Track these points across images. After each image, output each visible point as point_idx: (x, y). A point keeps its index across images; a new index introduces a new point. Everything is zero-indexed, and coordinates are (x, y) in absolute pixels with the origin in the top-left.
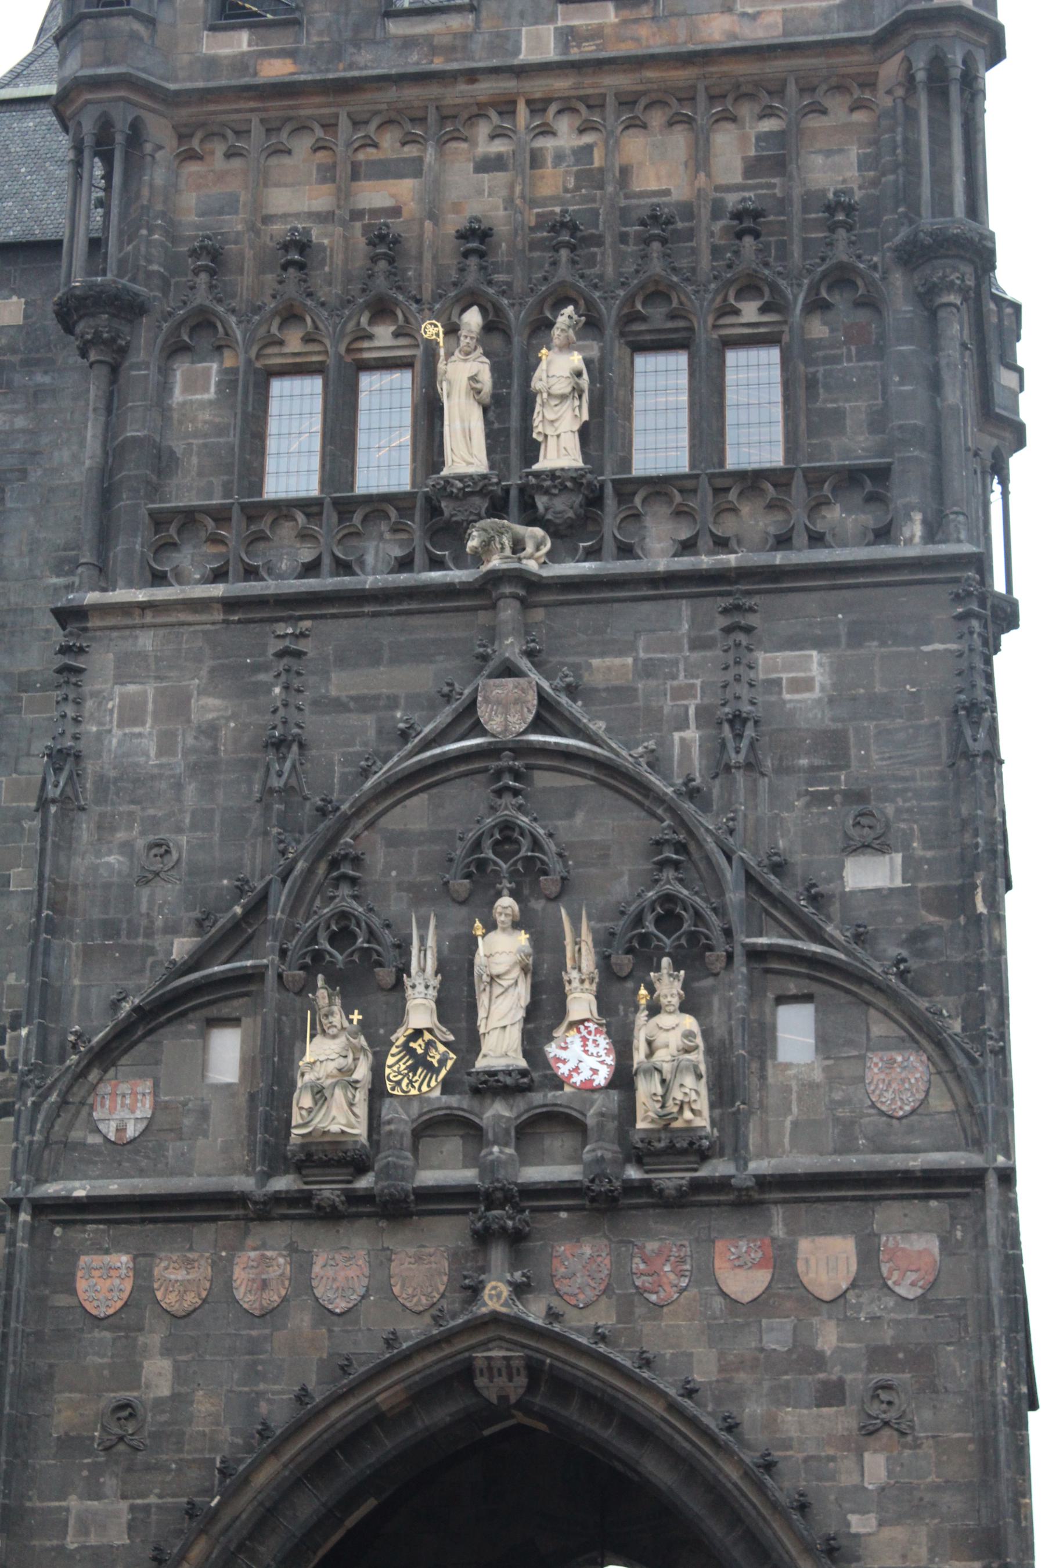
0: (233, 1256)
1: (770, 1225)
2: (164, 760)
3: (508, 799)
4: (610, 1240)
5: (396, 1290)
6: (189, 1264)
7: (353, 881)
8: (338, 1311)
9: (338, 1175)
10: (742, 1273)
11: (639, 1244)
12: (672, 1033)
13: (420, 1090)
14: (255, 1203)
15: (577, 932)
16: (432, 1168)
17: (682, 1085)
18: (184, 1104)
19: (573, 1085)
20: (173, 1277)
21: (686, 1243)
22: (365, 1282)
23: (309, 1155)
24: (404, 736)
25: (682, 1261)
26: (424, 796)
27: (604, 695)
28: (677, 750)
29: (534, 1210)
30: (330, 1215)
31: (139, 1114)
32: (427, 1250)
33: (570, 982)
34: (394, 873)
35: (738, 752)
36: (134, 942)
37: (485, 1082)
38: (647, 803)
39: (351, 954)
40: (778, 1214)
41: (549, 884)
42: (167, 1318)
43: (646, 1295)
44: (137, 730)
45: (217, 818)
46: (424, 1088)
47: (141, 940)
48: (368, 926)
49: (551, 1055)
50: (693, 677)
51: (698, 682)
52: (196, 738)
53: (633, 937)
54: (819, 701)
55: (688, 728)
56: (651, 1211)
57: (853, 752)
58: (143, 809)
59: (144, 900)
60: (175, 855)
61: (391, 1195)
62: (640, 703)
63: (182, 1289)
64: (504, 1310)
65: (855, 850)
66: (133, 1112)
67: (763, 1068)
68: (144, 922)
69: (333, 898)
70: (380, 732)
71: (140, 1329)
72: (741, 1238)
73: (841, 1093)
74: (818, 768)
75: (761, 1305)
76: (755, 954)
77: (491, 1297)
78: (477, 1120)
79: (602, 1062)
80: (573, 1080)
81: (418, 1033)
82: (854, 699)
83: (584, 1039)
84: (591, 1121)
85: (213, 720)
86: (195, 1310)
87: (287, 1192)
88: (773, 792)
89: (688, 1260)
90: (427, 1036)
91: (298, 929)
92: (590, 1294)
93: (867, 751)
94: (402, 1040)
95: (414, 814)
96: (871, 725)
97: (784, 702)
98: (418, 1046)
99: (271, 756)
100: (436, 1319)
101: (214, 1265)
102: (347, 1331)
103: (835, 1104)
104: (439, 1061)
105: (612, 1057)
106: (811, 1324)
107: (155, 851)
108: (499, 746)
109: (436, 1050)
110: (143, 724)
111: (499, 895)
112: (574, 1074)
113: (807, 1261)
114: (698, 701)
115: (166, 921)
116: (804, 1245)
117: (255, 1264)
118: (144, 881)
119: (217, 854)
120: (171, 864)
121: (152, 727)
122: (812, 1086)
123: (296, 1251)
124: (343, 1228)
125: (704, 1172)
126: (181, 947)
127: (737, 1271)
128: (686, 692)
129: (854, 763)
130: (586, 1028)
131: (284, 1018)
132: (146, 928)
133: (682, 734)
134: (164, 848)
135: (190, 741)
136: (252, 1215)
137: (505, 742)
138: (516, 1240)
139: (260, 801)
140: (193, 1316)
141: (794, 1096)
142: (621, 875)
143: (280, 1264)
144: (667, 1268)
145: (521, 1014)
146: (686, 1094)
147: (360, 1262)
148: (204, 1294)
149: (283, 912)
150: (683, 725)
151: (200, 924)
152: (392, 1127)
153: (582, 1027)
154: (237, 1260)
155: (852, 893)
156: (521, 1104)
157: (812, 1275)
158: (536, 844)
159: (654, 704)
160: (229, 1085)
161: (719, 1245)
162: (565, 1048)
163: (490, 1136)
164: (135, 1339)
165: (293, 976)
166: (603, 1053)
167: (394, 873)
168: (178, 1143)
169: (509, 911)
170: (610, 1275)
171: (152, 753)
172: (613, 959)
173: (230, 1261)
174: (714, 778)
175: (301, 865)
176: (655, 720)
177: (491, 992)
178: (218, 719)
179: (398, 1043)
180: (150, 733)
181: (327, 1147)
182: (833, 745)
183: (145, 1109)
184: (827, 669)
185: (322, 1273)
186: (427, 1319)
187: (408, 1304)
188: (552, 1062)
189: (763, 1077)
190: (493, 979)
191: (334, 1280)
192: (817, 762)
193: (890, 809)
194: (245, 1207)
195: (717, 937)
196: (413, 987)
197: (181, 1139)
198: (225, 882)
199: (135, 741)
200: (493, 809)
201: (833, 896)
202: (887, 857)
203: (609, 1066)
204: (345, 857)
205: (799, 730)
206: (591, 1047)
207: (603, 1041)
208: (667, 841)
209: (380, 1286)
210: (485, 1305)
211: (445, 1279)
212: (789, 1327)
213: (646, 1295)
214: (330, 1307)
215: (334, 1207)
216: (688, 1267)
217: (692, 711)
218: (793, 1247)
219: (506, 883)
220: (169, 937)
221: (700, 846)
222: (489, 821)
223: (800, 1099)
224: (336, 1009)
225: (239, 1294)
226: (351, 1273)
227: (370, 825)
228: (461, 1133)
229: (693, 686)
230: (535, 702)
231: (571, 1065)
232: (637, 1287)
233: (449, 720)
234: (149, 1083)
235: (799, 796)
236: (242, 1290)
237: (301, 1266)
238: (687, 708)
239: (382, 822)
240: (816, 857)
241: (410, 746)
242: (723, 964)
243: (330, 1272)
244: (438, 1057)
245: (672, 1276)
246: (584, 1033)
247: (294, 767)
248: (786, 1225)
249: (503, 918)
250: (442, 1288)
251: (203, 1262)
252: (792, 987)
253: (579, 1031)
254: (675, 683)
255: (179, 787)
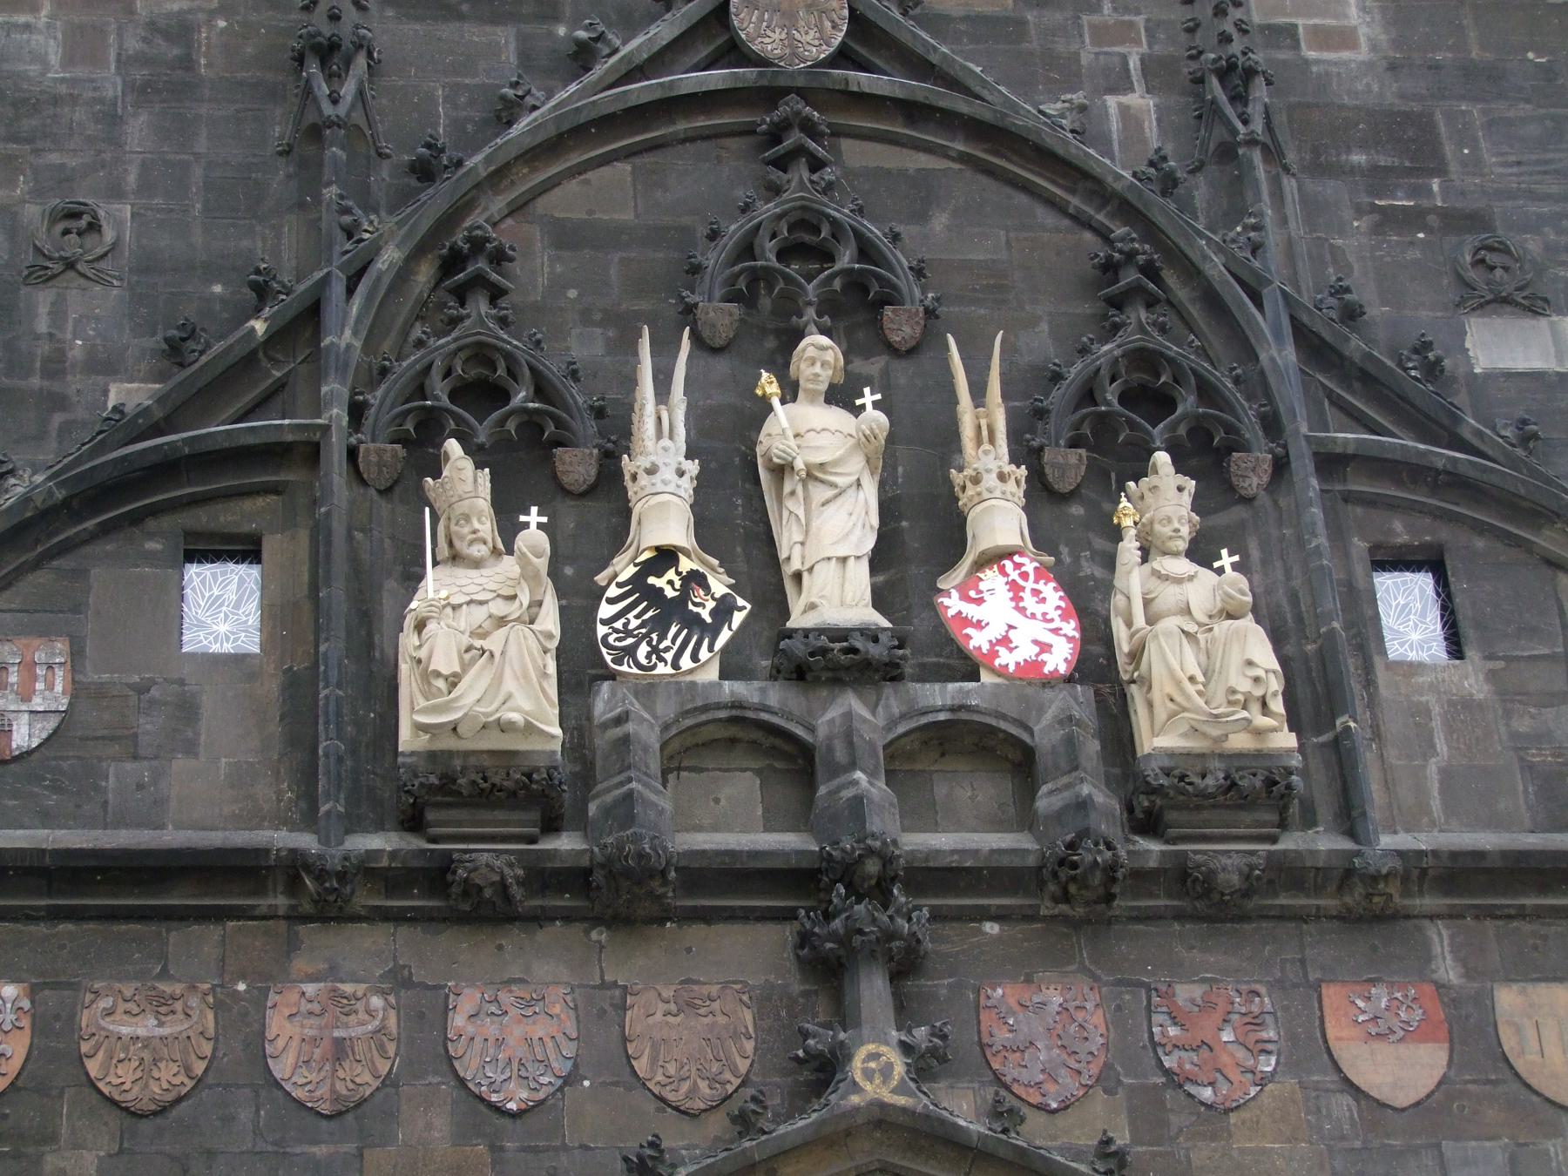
0: (265, 993)
1: (1429, 958)
2: (80, 72)
3: (801, 171)
4: (1096, 979)
5: (641, 1066)
6: (161, 1005)
7: (496, 294)
8: (512, 1106)
9: (506, 824)
10: (1383, 1050)
11: (1163, 988)
12: (1188, 586)
13: (675, 665)
14: (321, 875)
15: (978, 393)
16: (699, 829)
17: (1250, 663)
18: (142, 689)
19: (1001, 672)
20: (125, 1030)
21: (1262, 990)
22: (569, 1050)
23: (448, 780)
24: (583, 56)
25: (1256, 1022)
26: (623, 168)
27: (963, 27)
28: (1115, 125)
29: (937, 916)
30: (483, 910)
31: (38, 703)
32: (705, 990)
33: (976, 480)
34: (572, 294)
35: (1245, 122)
36: (22, 384)
37: (824, 651)
38: (1075, 202)
39: (502, 422)
40: (1440, 938)
41: (901, 325)
42: (114, 1119)
43: (1188, 1087)
44: (22, 19)
45: (198, 173)
46: (686, 662)
47: (36, 382)
48: (532, 369)
49: (951, 613)
50: (1127, 10)
51: (1140, 20)
52: (144, 39)
53: (1082, 420)
54: (1370, 65)
55: (1132, 90)
56: (1177, 926)
57: (1448, 149)
58: (37, 152)
59: (43, 310)
60: (109, 235)
61: (641, 855)
62: (1035, 45)
63: (147, 1055)
64: (901, 1101)
65: (1481, 306)
66: (27, 699)
67: (1368, 669)
68: (44, 348)
69: (454, 322)
70: (525, 58)
71: (51, 1138)
72: (1372, 982)
73: (1527, 721)
74: (1388, 170)
75: (1434, 1114)
76: (1330, 463)
77: (868, 1074)
78: (800, 732)
79: (1056, 631)
80: (997, 662)
81: (666, 557)
82: (1435, 67)
83: (1015, 588)
84: (1044, 735)
85: (181, 12)
86: (179, 1100)
87: (394, 854)
88: (1313, 209)
89: (1269, 1019)
90: (686, 565)
91: (384, 372)
92: (1070, 1085)
93: (1475, 148)
94: (631, 570)
95: (605, 192)
96: (1475, 112)
97: (1307, 62)
98: (666, 583)
99: (313, 68)
100: (744, 1123)
101: (218, 1007)
102: (535, 1150)
103: (1520, 743)
104: (713, 613)
105: (1073, 624)
106: (1547, 1152)
107: (60, 227)
108: (782, 82)
109: (707, 588)
110: (35, 9)
111: (799, 335)
112: (1002, 651)
113: (1518, 1030)
114: (1145, 48)
115: (90, 351)
116: (1507, 998)
117: (316, 1007)
118: (40, 275)
119: (198, 238)
120: (100, 251)
121: (52, 16)
122: (1468, 704)
123: (408, 983)
124: (512, 939)
125: (1289, 842)
126: (129, 393)
127: (1377, 1045)
128: (1125, 33)
129: (1453, 167)
130: (1018, 566)
131: (358, 535)
132: (46, 361)
133: (1123, 99)
134: (86, 219)
135: (133, 45)
136: (307, 907)
137: (792, 75)
138: (905, 966)
139: (287, 153)
140: (175, 1113)
141: (1437, 723)
142: (1033, 322)
143: (377, 1010)
144: (1227, 1036)
145: (870, 543)
146: (1257, 680)
147: (557, 1009)
148: (199, 1068)
149: (355, 333)
150: (1121, 84)
151: (175, 351)
152: (630, 727)
153: (1008, 564)
154: (273, 998)
155: (1490, 376)
156: (893, 700)
157: (1532, 1056)
158: (866, 250)
159: (1060, 47)
160: (238, 659)
161: (1331, 994)
162: (980, 601)
163: (840, 755)
164: (38, 1161)
165: (379, 452)
166: (1055, 615)
167: (572, 294)
168: (129, 766)
169: (829, 356)
170: (1106, 1045)
171: (54, 59)
172: (1048, 456)
173: (259, 1001)
174: (1192, 172)
175: (390, 256)
176: (1067, 74)
177: (806, 499)
178: (190, 11)
179: (622, 578)
180: (48, 26)
181: (487, 762)
182: (1411, 141)
183: (53, 693)
184: (1378, 17)
185: (471, 1029)
186: (717, 1125)
187: (671, 1097)
188: (953, 629)
189: (1369, 682)
190: (813, 475)
191: (499, 1042)
192: (1383, 161)
193: (1533, 245)
194: (293, 885)
195: (1251, 429)
196: (652, 471)
197: (135, 757)
198: (218, 289)
199: (16, 36)
200: (775, 190)
201: (1454, 379)
202: (1543, 323)
203: (1070, 639)
204: (478, 244)
205: (1342, 107)
206: (1029, 601)
207: (1053, 596)
208: (1130, 256)
209: (607, 1056)
210: (856, 1087)
211: (749, 1046)
212: (1501, 1158)
213: (1188, 1087)
214: (494, 1098)
215: (503, 887)
216: (1272, 1034)
217: (1134, 63)
218: (1484, 1003)
219: (811, 313)
220: (100, 379)
221: (1191, 272)
222: (767, 210)
223: (1450, 730)
224: (484, 503)
225: (280, 1069)
226: (539, 1030)
227: (517, 209)
228: (756, 765)
229: (1131, 24)
230: (846, 12)
231: (995, 631)
232: (1167, 1072)
233: (676, 32)
234: (61, 645)
235: (1359, 211)
236: (290, 1059)
237: (421, 1015)
238: (1124, 59)
239: (541, 205)
240: (1407, 312)
241: (589, 78)
242: (1266, 479)
243: (491, 1028)
244: (711, 604)
245: (1241, 1054)
246: (1014, 575)
247: (361, 93)
248: (1462, 961)
249: (817, 369)
250: (743, 1066)
251: (194, 1001)
252: (1401, 532)
253: (1005, 574)
254: (1096, 18)
255: (112, 119)
